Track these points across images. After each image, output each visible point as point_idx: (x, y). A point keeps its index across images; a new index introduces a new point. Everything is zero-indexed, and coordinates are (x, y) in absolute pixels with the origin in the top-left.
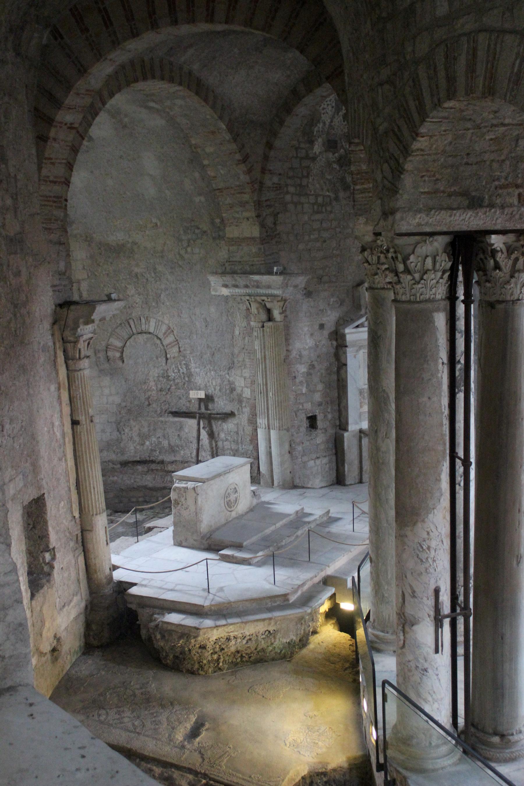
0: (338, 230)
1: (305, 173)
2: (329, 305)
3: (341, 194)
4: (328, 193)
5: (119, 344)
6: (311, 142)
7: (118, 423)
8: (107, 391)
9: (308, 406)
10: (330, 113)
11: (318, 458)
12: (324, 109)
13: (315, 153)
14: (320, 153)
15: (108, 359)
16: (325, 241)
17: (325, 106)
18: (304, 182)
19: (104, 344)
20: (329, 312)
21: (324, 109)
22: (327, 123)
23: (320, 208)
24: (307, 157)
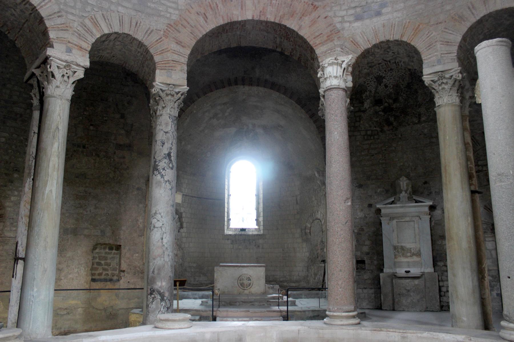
0: (383, 148)
1: (358, 119)
2: (376, 192)
3: (386, 128)
5: (309, 226)
6: (362, 103)
7: (308, 267)
8: (304, 250)
10: (374, 86)
11: (365, 288)
12: (368, 84)
14: (369, 107)
15: (306, 233)
18: (357, 124)
19: (304, 225)
20: (376, 197)
21: (368, 84)
22: (373, 92)
23: (369, 137)
24: (360, 111)
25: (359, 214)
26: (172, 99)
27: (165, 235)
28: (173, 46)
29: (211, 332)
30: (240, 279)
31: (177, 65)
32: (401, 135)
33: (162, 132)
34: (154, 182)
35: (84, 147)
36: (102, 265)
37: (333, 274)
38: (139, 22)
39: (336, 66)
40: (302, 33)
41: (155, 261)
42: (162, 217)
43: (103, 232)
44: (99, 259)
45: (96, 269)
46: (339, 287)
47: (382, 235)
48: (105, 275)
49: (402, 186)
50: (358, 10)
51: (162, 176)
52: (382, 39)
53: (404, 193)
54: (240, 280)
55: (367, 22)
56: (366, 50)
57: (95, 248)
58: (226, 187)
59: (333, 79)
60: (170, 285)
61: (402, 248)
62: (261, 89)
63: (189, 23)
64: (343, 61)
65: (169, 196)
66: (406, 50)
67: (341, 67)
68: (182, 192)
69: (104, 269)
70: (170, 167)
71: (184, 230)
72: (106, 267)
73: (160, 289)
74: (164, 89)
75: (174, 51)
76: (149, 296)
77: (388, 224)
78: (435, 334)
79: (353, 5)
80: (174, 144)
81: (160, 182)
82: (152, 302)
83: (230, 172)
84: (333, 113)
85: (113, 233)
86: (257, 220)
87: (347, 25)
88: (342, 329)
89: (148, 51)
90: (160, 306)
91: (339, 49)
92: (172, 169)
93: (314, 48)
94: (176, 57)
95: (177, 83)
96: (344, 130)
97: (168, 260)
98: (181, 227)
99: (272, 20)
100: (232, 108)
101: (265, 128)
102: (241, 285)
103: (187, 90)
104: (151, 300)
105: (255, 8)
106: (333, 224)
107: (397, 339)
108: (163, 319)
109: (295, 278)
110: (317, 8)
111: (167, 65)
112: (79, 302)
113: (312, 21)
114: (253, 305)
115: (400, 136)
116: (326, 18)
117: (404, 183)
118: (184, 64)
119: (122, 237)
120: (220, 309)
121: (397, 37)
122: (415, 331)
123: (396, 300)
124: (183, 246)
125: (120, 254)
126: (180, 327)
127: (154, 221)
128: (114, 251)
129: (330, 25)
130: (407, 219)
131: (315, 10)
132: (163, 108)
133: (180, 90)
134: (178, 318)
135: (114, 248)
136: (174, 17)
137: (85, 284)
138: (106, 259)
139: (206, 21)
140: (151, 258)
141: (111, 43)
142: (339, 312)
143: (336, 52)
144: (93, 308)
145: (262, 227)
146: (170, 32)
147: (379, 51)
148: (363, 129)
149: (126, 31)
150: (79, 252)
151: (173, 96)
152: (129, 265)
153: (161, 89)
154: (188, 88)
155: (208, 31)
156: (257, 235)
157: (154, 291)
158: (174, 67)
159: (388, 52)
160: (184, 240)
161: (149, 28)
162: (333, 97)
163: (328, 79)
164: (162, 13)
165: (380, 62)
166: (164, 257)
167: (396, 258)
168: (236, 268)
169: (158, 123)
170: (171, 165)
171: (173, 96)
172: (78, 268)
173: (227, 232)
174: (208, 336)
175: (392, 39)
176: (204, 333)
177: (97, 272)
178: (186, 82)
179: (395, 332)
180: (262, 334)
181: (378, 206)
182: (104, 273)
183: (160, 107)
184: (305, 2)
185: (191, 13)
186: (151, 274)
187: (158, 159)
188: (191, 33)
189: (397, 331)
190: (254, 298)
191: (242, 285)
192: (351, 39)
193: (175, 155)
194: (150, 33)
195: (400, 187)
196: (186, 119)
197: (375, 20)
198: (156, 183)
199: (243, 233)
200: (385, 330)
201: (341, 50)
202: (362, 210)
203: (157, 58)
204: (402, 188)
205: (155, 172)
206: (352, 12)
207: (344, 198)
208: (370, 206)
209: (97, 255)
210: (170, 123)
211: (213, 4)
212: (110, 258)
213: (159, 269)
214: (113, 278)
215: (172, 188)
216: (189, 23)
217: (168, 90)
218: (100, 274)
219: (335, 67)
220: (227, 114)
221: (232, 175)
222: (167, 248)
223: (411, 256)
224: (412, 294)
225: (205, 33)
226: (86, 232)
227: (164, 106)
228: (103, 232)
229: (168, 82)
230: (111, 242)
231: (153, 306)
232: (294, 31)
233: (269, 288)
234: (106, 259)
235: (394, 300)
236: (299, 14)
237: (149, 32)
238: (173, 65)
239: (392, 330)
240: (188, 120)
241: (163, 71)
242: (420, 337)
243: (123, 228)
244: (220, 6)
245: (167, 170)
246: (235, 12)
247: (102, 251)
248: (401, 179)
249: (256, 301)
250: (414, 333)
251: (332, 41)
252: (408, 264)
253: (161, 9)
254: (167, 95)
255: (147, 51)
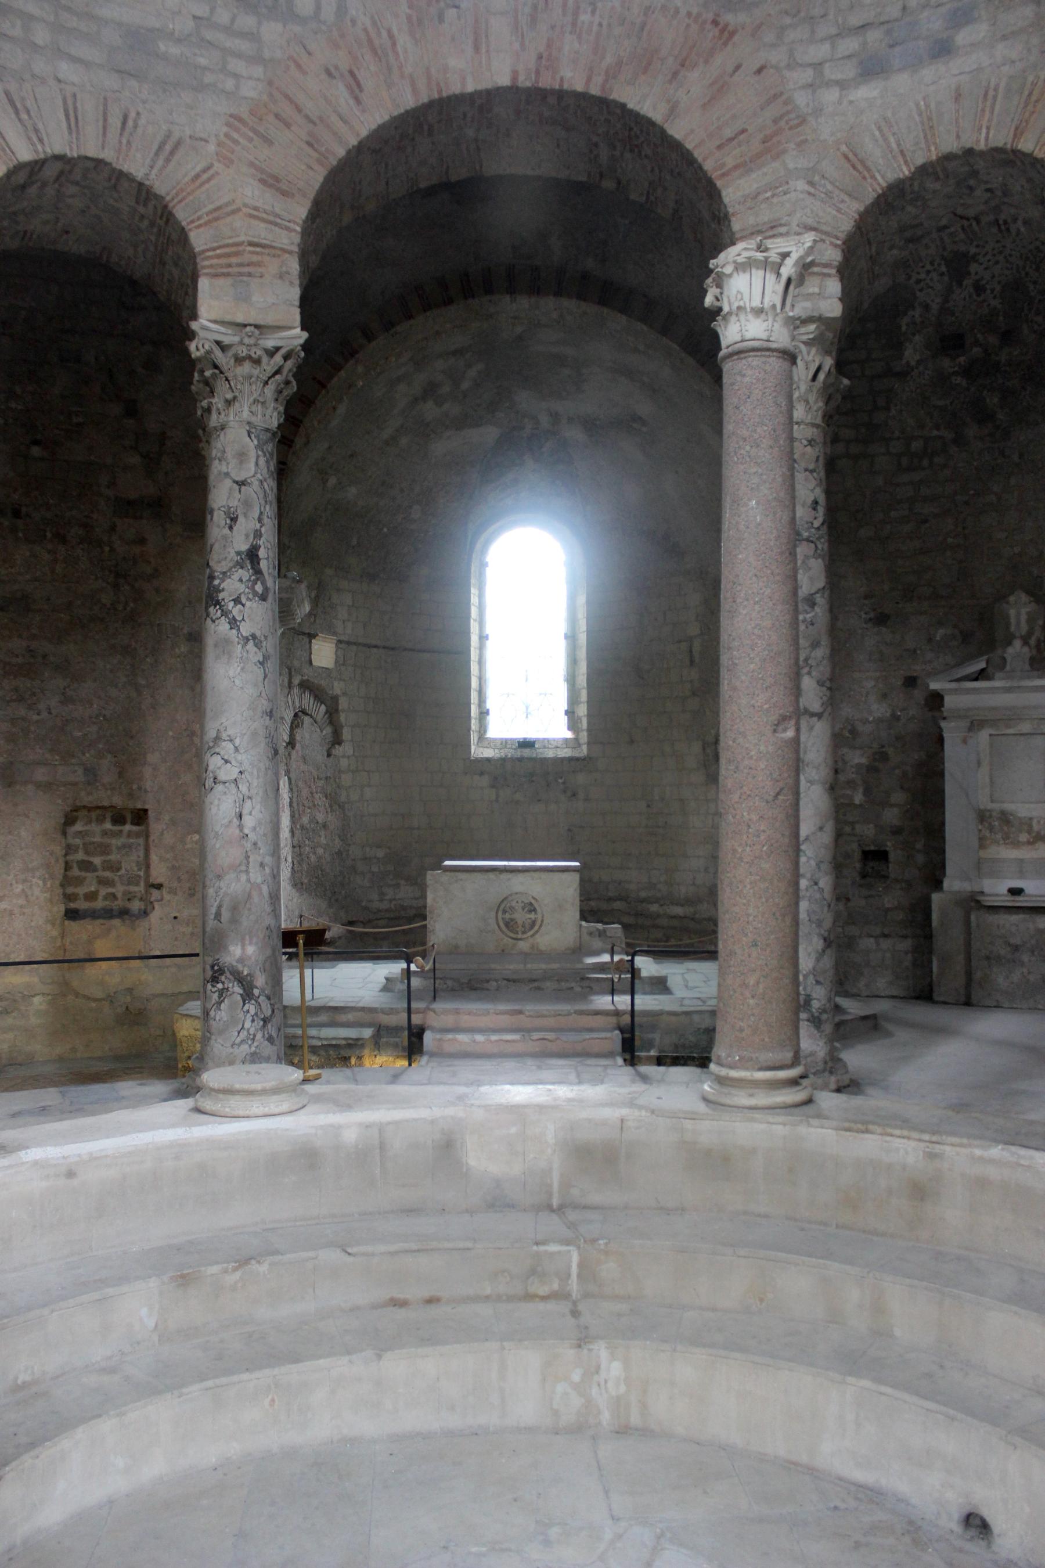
2: (930, 640)
4: (935, 433)
9: (868, 830)
11: (886, 936)
12: (918, 281)
13: (908, 363)
14: (919, 362)
16: (926, 521)
17: (923, 276)
20: (929, 655)
21: (918, 281)
22: (935, 308)
25: (875, 707)
26: (256, 372)
27: (248, 804)
28: (252, 193)
29: (360, 1124)
30: (503, 906)
31: (266, 259)
32: (1021, 456)
33: (228, 483)
34: (210, 641)
35: (17, 514)
36: (95, 870)
37: (732, 953)
38: (133, 115)
39: (761, 273)
40: (676, 130)
41: (222, 884)
42: (237, 749)
43: (91, 772)
44: (87, 853)
45: (79, 881)
46: (748, 994)
47: (942, 774)
48: (105, 898)
49: (1013, 621)
50: (874, 36)
51: (234, 623)
52: (949, 144)
53: (1017, 643)
54: (505, 912)
55: (901, 81)
56: (891, 187)
57: (69, 820)
58: (474, 612)
59: (750, 316)
60: (269, 952)
61: (1005, 818)
62: (569, 304)
63: (299, 110)
64: (785, 255)
65: (256, 685)
66: (1030, 180)
67: (778, 274)
68: (334, 634)
69: (103, 882)
70: (255, 594)
71: (346, 749)
72: (107, 874)
73: (240, 967)
74: (226, 340)
75: (256, 209)
76: (209, 986)
77: (965, 741)
78: (1023, 1152)
79: (855, 20)
80: (266, 520)
81: (227, 641)
82: (219, 1003)
83: (486, 565)
84: (745, 433)
85: (121, 774)
86: (570, 713)
87: (830, 96)
88: (753, 1120)
89: (171, 214)
90: (241, 1015)
91: (801, 185)
92: (263, 598)
93: (719, 183)
94: (261, 232)
95: (269, 319)
96: (782, 494)
97: (259, 880)
98: (337, 740)
99: (579, 87)
100: (480, 366)
101: (590, 425)
102: (507, 925)
103: (302, 341)
104: (215, 996)
105: (522, 45)
106: (735, 797)
107: (911, 1160)
108: (216, 1086)
109: (683, 889)
110: (732, 34)
111: (234, 260)
112: (36, 980)
113: (712, 85)
114: (539, 988)
115: (1016, 458)
116: (759, 71)
117: (1019, 611)
118: (290, 252)
119: (148, 785)
120: (434, 1006)
121: (1001, 138)
122: (965, 1141)
123: (978, 975)
124: (343, 798)
125: (147, 837)
126: (266, 1110)
127: (214, 762)
128: (128, 827)
129: (775, 97)
130: (1026, 727)
131: (725, 44)
132: (229, 403)
133: (279, 344)
134: (259, 1087)
135: (129, 819)
136: (250, 90)
137: (49, 927)
138: (105, 850)
139: (358, 101)
140: (210, 876)
141: (50, 191)
142: (747, 1069)
143: (793, 196)
144: (77, 995)
145: (584, 737)
146: (236, 142)
147: (937, 186)
148: (897, 434)
149: (92, 151)
150: (23, 833)
151: (257, 362)
152: (174, 867)
153: (218, 343)
154: (305, 335)
155: (364, 133)
156: (571, 759)
157: (221, 971)
158: (259, 264)
159: (971, 189)
160: (346, 779)
161: (168, 135)
162: (747, 379)
163: (733, 318)
164: (209, 78)
165: (944, 222)
166: (247, 872)
167: (982, 846)
168: (491, 875)
169: (214, 453)
170: (259, 588)
171: (257, 362)
172: (25, 881)
173: (477, 751)
174: (350, 1136)
175: (982, 146)
176: (337, 1128)
177: (81, 891)
178: (295, 316)
179: (909, 1138)
180: (513, 1130)
181: (934, 686)
182: (103, 891)
183: (217, 402)
184: (689, 14)
185: (304, 73)
186: (211, 923)
187: (219, 568)
188: (308, 143)
189: (915, 1135)
190: (544, 966)
191: (510, 925)
192: (844, 148)
193: (273, 553)
194: (172, 153)
195: (1008, 625)
196: (334, 408)
197: (928, 73)
198: (216, 646)
199: (527, 753)
200: (879, 1130)
201: (807, 188)
202: (885, 696)
203: (199, 240)
204: (1013, 629)
205: (212, 610)
206: (850, 45)
207: (774, 718)
208: (911, 682)
209: (78, 841)
210: (253, 453)
211: (379, 34)
212: (119, 848)
213: (234, 908)
214: (128, 905)
215: (266, 658)
216: (299, 110)
217: (241, 343)
218: (91, 896)
219: (758, 274)
220: (465, 385)
221: (489, 572)
222: (255, 844)
223: (1029, 843)
224: (1025, 958)
225: (356, 143)
226: (41, 774)
227: (229, 396)
228: (91, 772)
229: (240, 319)
230: (118, 801)
231: (221, 1015)
232: (651, 123)
233: (591, 934)
234: (105, 850)
235: (969, 974)
236: (671, 60)
237: (169, 148)
238: (255, 258)
239: (898, 1132)
240: (342, 409)
241: (221, 281)
242: (981, 1159)
243: (153, 758)
244: (403, 40)
245: (248, 604)
246: (453, 62)
247: (95, 828)
248: (1012, 599)
249: (546, 977)
250: (961, 1145)
251: (777, 156)
252: (1021, 868)
253: (203, 61)
254: (239, 360)
255: (166, 215)
